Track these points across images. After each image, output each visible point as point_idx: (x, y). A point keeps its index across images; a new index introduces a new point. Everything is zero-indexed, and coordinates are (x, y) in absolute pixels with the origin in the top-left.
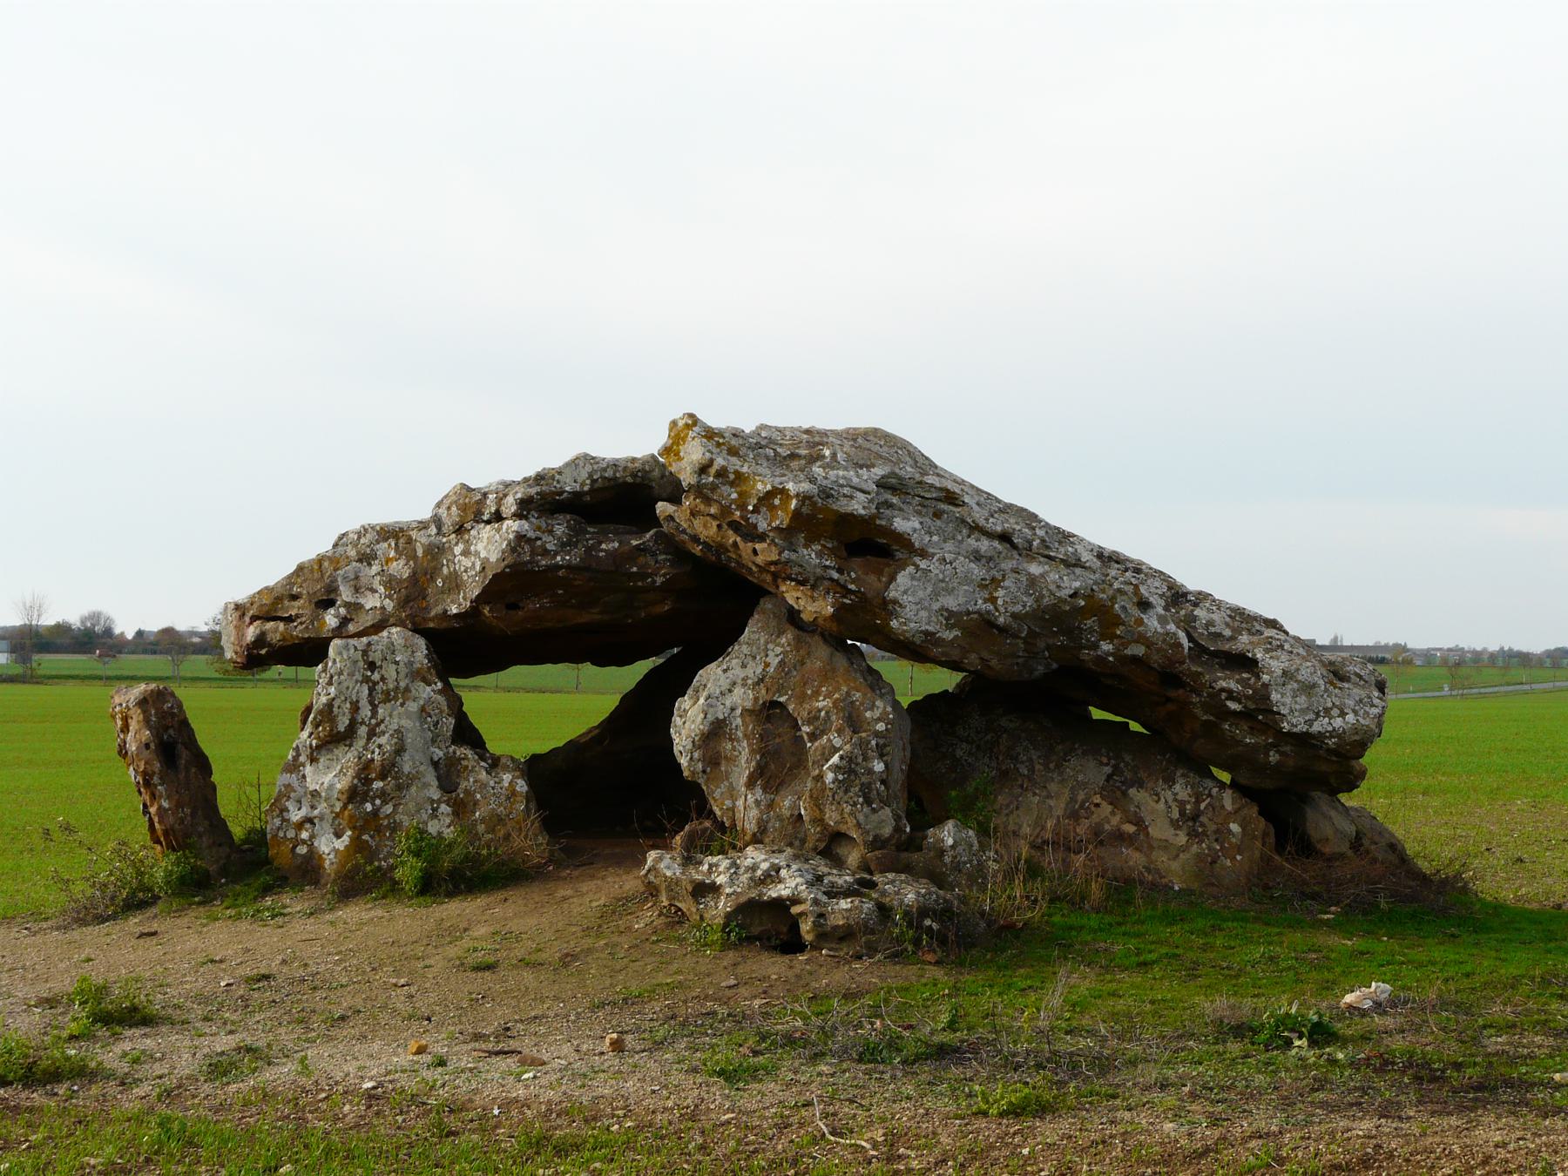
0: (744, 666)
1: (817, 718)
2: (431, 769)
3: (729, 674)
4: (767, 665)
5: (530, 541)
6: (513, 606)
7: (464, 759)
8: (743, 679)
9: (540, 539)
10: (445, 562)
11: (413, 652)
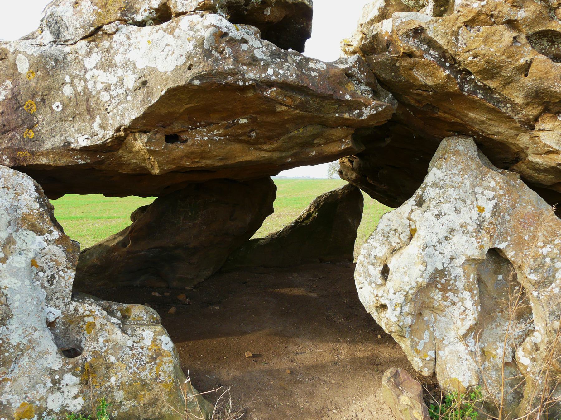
0: (457, 211)
1: (542, 265)
2: (48, 334)
3: (443, 219)
4: (481, 210)
5: (232, 42)
6: (172, 138)
7: (88, 316)
8: (462, 226)
9: (246, 41)
10: (68, 79)
11: (17, 194)
